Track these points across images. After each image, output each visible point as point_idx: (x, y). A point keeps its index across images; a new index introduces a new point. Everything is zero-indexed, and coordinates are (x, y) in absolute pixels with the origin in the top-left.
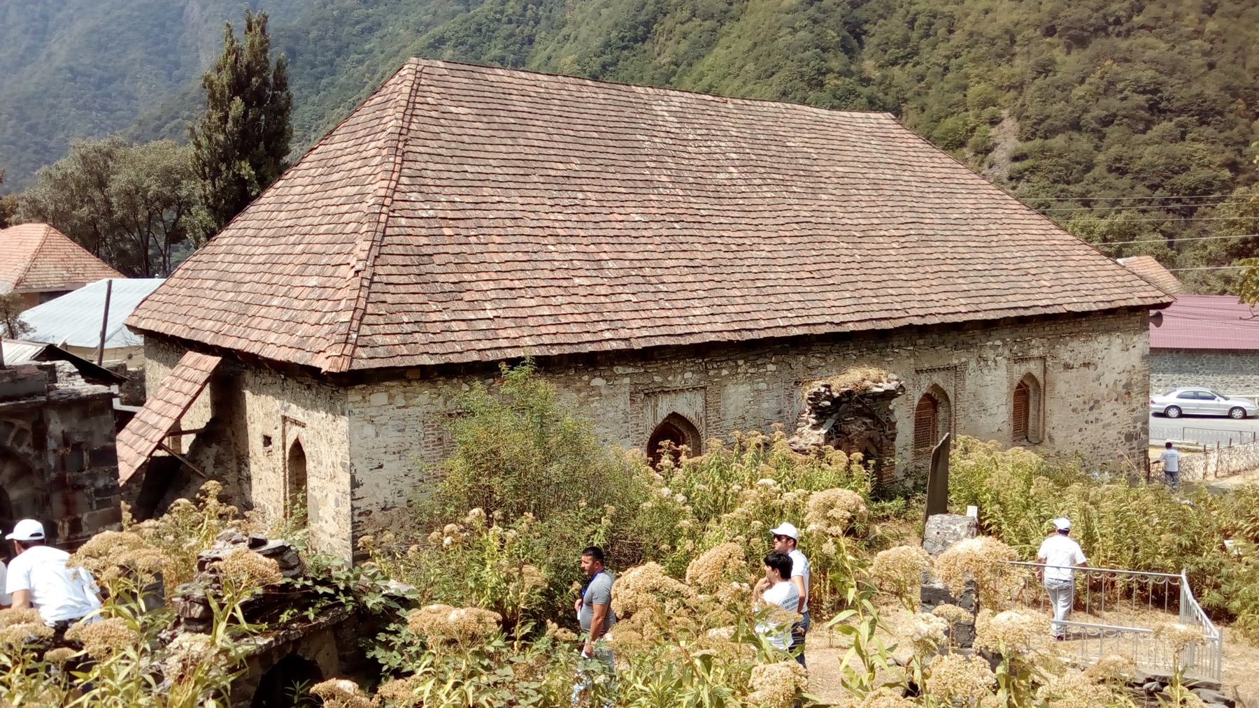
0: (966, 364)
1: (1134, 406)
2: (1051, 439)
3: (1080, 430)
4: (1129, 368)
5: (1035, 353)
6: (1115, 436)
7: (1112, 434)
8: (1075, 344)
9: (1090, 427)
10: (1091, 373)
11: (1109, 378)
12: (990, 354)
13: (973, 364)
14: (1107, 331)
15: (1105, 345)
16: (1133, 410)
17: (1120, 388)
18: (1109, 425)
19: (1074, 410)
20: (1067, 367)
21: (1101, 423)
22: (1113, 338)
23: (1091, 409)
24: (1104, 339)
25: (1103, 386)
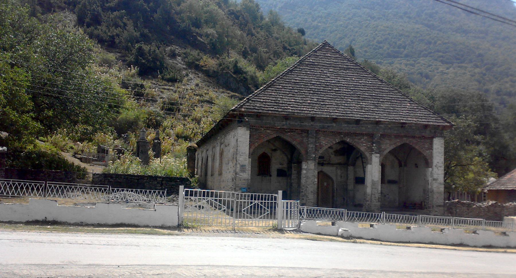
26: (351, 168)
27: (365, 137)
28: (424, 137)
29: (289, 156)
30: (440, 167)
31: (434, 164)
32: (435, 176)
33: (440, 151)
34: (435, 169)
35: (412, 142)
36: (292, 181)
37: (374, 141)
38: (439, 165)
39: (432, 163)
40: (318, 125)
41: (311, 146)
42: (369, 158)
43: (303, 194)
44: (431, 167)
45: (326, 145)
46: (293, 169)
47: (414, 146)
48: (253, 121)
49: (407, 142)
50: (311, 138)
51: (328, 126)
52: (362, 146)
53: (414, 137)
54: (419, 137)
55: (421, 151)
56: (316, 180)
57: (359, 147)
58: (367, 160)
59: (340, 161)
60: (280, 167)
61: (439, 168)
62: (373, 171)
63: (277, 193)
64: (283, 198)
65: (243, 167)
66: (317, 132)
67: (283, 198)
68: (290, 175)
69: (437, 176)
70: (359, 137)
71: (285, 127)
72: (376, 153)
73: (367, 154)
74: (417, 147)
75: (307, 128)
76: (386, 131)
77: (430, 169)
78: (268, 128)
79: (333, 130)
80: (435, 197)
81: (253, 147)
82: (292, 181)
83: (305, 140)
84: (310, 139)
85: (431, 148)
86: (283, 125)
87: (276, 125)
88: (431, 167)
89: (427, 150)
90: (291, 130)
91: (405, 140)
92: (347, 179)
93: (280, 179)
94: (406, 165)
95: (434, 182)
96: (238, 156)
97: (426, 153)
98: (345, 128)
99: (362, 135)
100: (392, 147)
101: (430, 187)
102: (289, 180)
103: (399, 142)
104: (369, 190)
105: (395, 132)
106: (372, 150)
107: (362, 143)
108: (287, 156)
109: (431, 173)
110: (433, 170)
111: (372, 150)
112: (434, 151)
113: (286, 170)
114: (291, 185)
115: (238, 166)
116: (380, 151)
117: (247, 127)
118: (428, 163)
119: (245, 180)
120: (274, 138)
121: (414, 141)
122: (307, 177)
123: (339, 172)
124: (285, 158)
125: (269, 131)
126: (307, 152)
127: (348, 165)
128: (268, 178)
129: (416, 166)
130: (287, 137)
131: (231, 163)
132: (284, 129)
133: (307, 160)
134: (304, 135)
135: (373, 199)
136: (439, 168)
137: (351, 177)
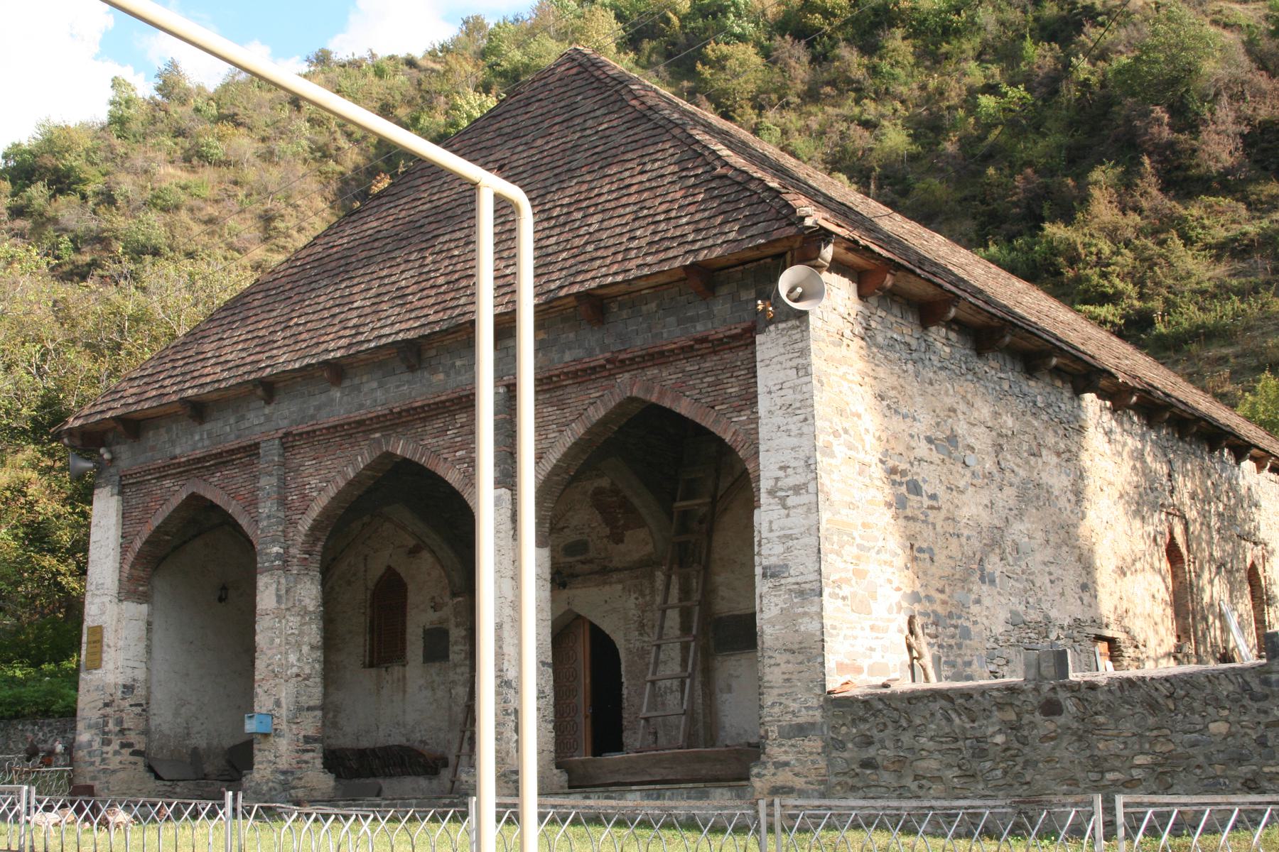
28: (717, 346)
38: (791, 481)
40: (285, 414)
45: (321, 490)
47: (667, 403)
49: (636, 392)
51: (318, 408)
53: (658, 358)
54: (687, 352)
57: (441, 470)
69: (779, 549)
70: (438, 424)
71: (199, 453)
74: (684, 408)
79: (333, 421)
81: (130, 557)
87: (178, 451)
91: (627, 385)
105: (568, 357)
112: (763, 404)
121: (669, 376)
123: (631, 602)
128: (396, 670)
132: (199, 459)
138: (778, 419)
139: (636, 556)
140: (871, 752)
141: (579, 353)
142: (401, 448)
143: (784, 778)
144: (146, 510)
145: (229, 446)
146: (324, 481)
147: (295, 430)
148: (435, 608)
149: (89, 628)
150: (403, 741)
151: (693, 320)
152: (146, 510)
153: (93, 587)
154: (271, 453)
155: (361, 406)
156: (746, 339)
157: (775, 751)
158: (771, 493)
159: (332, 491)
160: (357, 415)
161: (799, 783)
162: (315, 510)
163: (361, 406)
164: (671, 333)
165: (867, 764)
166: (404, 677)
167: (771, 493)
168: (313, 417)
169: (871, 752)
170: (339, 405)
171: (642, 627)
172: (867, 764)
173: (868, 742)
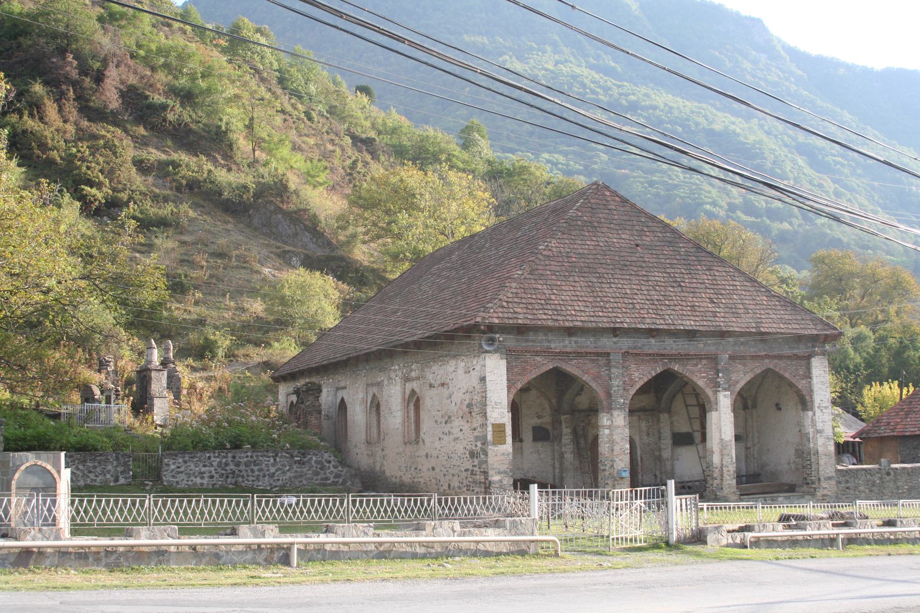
0: (383, 381)
1: (475, 425)
2: (423, 441)
3: (440, 439)
4: (471, 389)
5: (413, 374)
6: (462, 451)
7: (460, 448)
8: (435, 368)
9: (446, 438)
10: (445, 392)
11: (458, 397)
12: (393, 375)
13: (386, 382)
14: (455, 357)
15: (453, 368)
16: (475, 429)
17: (464, 407)
18: (457, 439)
19: (436, 421)
20: (431, 386)
21: (452, 437)
22: (459, 361)
23: (446, 423)
24: (453, 362)
25: (453, 404)
26: (664, 417)
27: (704, 362)
28: (797, 357)
29: (554, 401)
30: (826, 408)
31: (816, 405)
32: (820, 426)
33: (823, 379)
34: (818, 413)
35: (779, 366)
36: (564, 449)
37: (720, 367)
39: (812, 401)
40: (625, 343)
41: (615, 382)
42: (712, 399)
43: (607, 473)
44: (812, 410)
45: (640, 378)
46: (564, 425)
47: (781, 372)
48: (511, 341)
49: (771, 366)
50: (615, 367)
52: (700, 377)
53: (780, 357)
55: (794, 381)
56: (628, 446)
57: (695, 379)
58: (709, 402)
59: (644, 404)
60: (536, 421)
61: (824, 411)
62: (722, 423)
63: (666, 485)
64: (676, 494)
65: (499, 429)
66: (626, 354)
67: (676, 494)
68: (559, 438)
70: (694, 362)
71: (568, 350)
72: (725, 390)
73: (709, 392)
74: (787, 375)
75: (606, 350)
76: (737, 348)
77: (810, 413)
78: (537, 353)
79: (650, 352)
80: (822, 462)
81: (514, 391)
82: (564, 449)
83: (604, 372)
84: (613, 370)
85: (808, 375)
86: (565, 347)
87: (553, 346)
88: (812, 410)
89: (803, 379)
90: (579, 355)
91: (768, 364)
92: (660, 438)
93: (539, 445)
94: (754, 406)
95: (818, 435)
96: (489, 409)
97: (801, 384)
98: (671, 346)
99: (699, 357)
100: (748, 377)
101: (812, 445)
102: (556, 448)
103: (758, 368)
104: (716, 459)
106: (717, 385)
107: (700, 371)
108: (550, 400)
109: (812, 420)
110: (814, 414)
111: (717, 385)
112: (815, 380)
113: (549, 427)
114: (562, 456)
115: (490, 428)
116: (729, 386)
117: (501, 353)
118: (804, 402)
119: (503, 454)
120: (550, 370)
121: (782, 364)
122: (612, 442)
123: (643, 424)
124: (547, 406)
125: (538, 359)
126: (609, 395)
127: (660, 412)
129: (778, 407)
130: (571, 368)
131: (457, 423)
133: (610, 409)
134: (602, 361)
135: (725, 475)
136: (824, 411)
137: (667, 433)
138: (819, 385)
139: (638, 406)
140: (848, 485)
141: (755, 349)
142: (676, 368)
143: (825, 492)
144: (524, 369)
145: (589, 350)
146: (642, 374)
147: (631, 351)
148: (539, 417)
149: (493, 425)
150: (522, 477)
151: (794, 348)
152: (524, 369)
153: (493, 404)
154: (616, 358)
155: (665, 349)
156: (808, 358)
157: (824, 484)
158: (819, 407)
159: (646, 380)
160: (662, 352)
161: (829, 493)
162: (638, 386)
163: (665, 349)
164: (787, 351)
165: (848, 488)
166: (522, 448)
167: (819, 407)
168: (640, 348)
169: (848, 485)
170: (653, 345)
171: (648, 434)
172: (848, 488)
173: (847, 482)
